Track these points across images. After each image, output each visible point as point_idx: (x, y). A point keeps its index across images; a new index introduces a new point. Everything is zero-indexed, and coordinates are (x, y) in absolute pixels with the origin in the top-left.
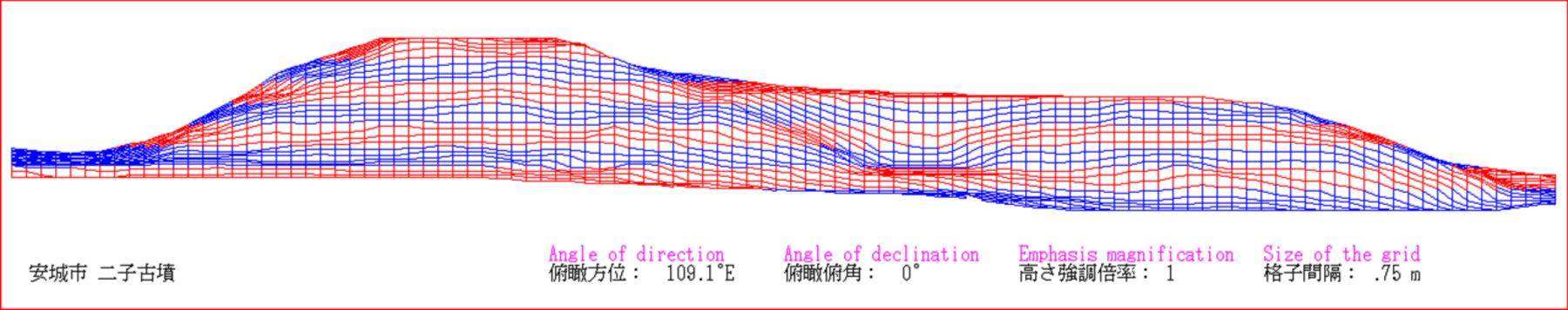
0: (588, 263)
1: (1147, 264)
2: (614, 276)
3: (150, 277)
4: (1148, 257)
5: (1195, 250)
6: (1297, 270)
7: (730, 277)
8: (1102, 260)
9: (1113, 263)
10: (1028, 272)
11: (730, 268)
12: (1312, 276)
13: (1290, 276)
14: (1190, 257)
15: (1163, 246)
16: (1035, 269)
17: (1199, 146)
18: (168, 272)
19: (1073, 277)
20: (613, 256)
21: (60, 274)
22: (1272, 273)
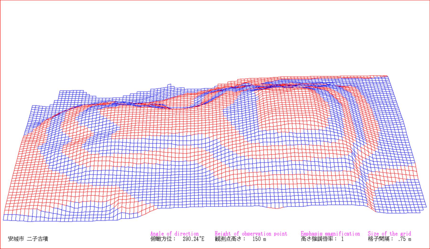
0: (161, 236)
1: (336, 236)
2: (168, 240)
3: (41, 240)
4: (336, 234)
5: (260, 233)
6: (377, 238)
7: (203, 240)
8: (324, 235)
9: (327, 236)
10: (303, 239)
11: (203, 238)
12: (381, 240)
13: (375, 240)
14: (348, 234)
15: (340, 232)
16: (305, 238)
17: (168, 115)
18: (46, 239)
19: (316, 240)
20: (168, 234)
21: (16, 239)
22: (370, 239)
